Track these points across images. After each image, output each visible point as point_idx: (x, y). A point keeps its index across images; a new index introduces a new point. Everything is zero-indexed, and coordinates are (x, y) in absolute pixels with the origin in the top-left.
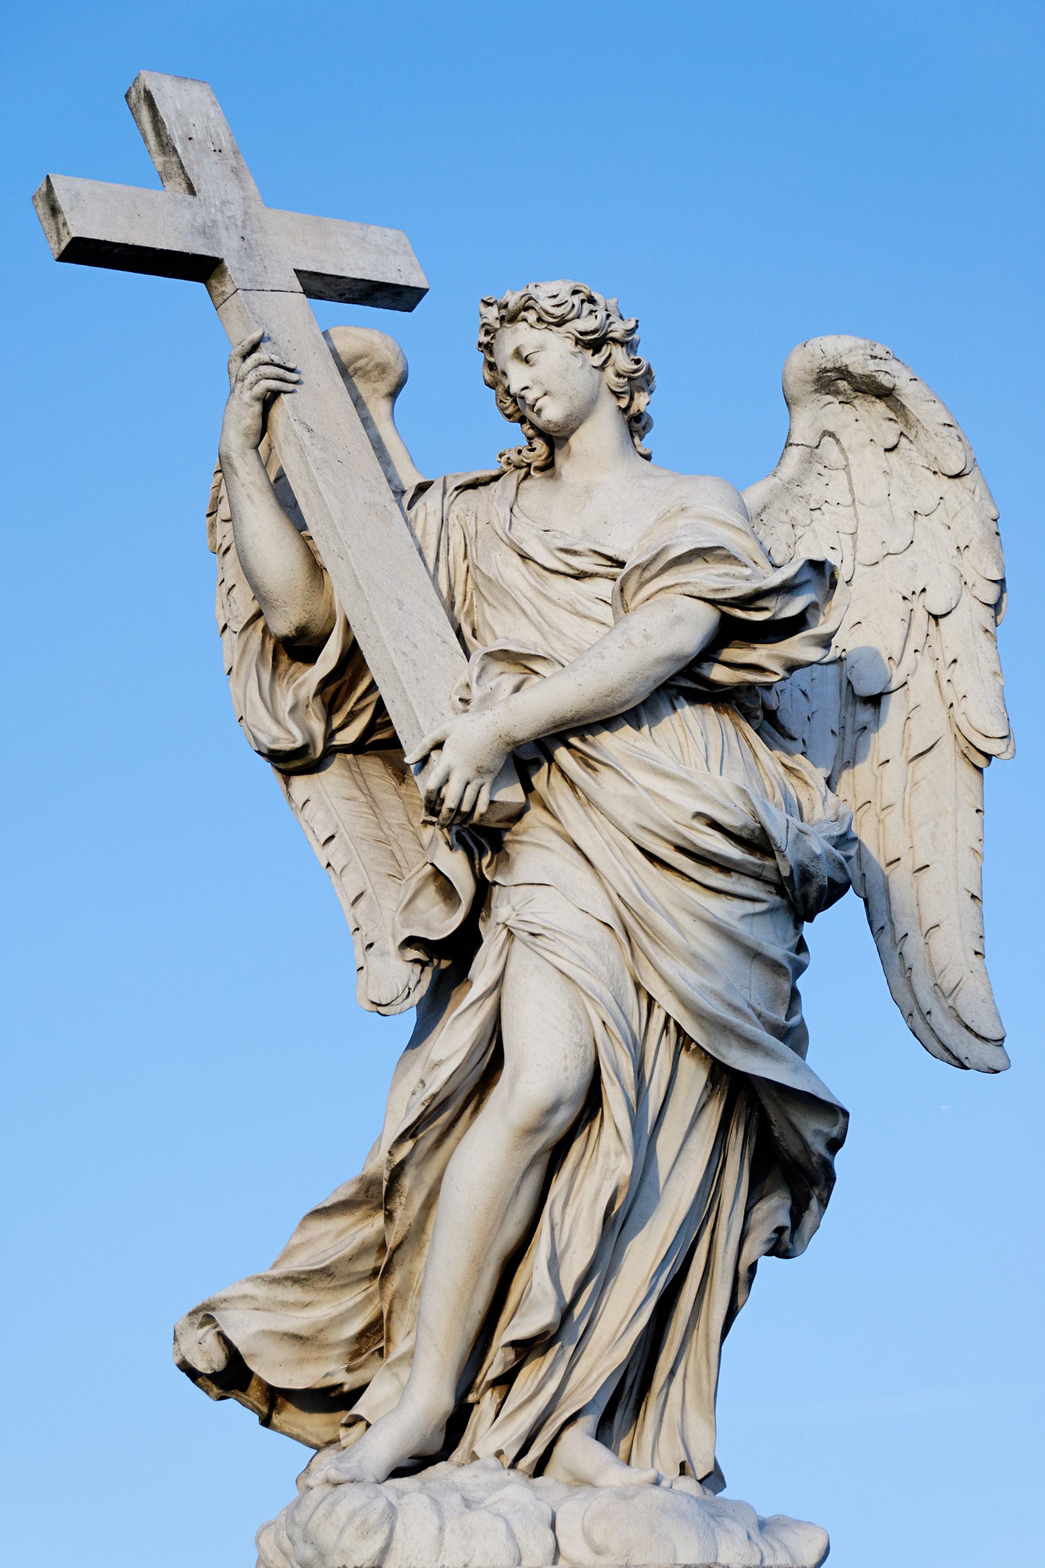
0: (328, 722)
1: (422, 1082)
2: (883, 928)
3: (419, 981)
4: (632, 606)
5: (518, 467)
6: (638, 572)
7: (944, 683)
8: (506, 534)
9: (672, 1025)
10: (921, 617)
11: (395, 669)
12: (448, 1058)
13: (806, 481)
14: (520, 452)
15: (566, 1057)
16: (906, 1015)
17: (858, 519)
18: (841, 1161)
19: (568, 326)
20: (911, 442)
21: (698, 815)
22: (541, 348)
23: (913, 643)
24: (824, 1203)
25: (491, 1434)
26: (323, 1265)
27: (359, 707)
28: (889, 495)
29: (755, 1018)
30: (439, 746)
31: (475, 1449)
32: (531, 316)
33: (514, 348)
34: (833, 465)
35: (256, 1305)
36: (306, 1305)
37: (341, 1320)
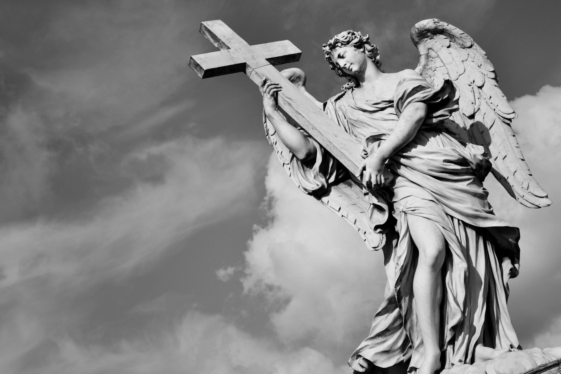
0: (326, 178)
1: (397, 264)
3: (383, 238)
4: (401, 111)
5: (349, 89)
6: (400, 100)
7: (490, 104)
8: (356, 106)
9: (460, 222)
10: (476, 89)
11: (342, 153)
17: (447, 69)
19: (351, 43)
20: (454, 42)
21: (445, 161)
22: (345, 52)
23: (477, 96)
25: (455, 356)
26: (386, 328)
30: (364, 169)
32: (339, 44)
33: (338, 55)
34: (434, 56)
35: (370, 347)
36: (384, 342)
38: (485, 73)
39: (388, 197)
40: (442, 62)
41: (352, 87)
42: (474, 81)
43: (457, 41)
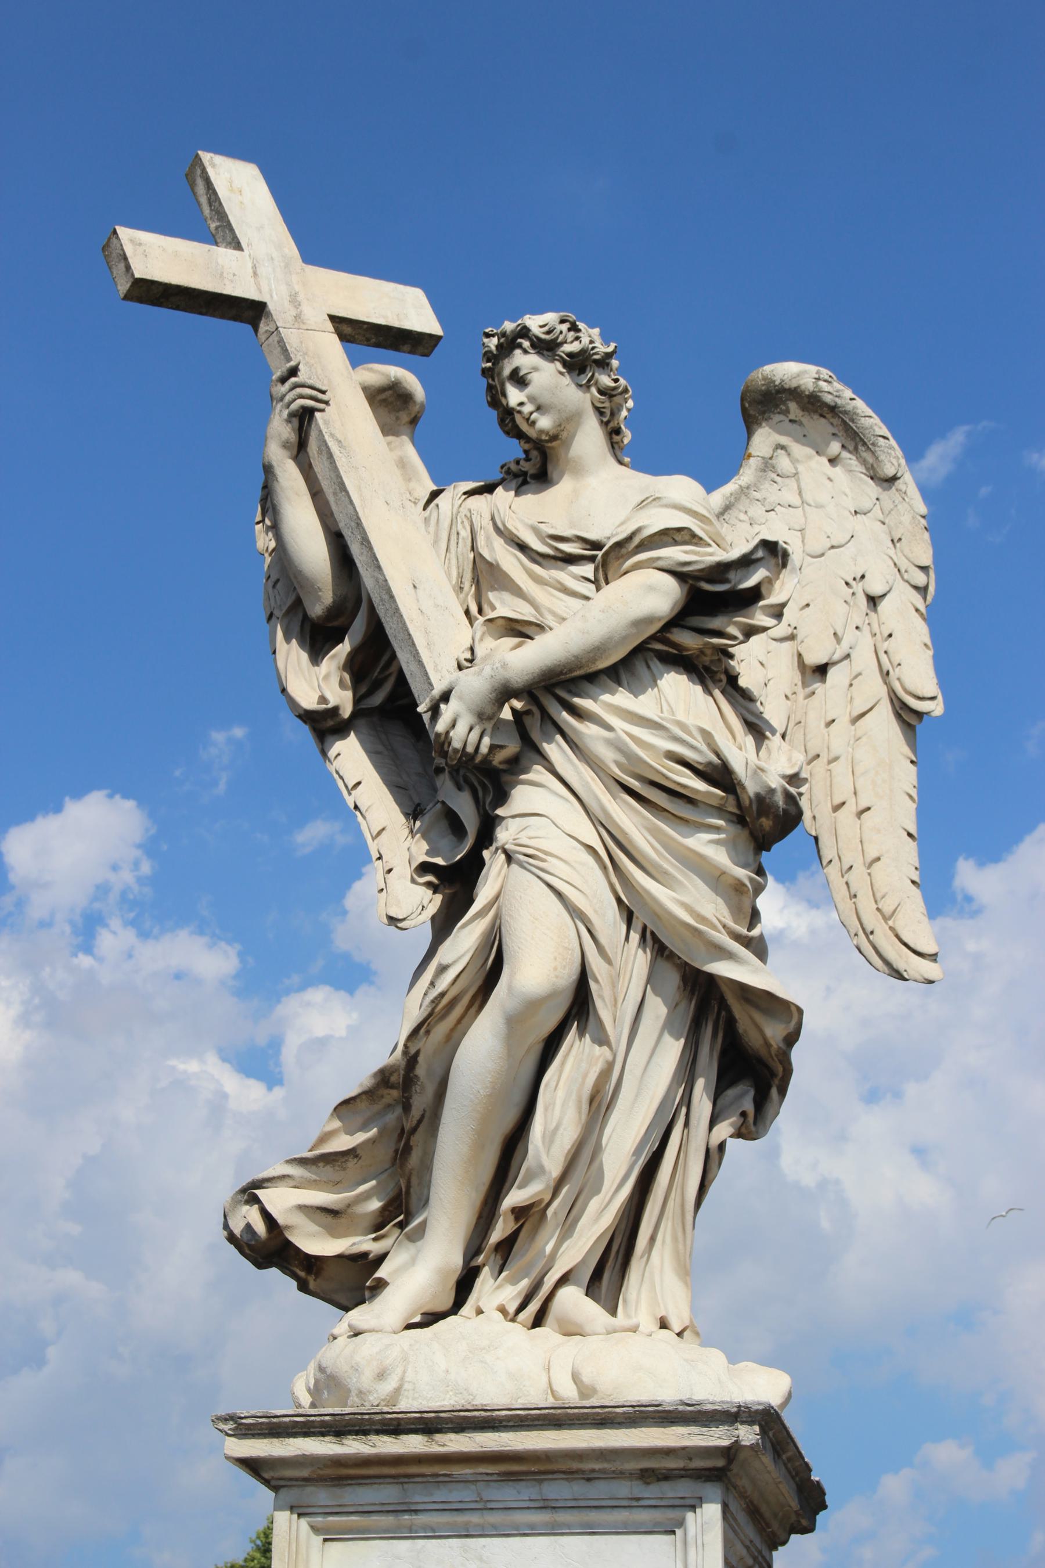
2: (831, 861)
10: (863, 601)
12: (455, 962)
13: (762, 487)
14: (518, 462)
15: (555, 959)
16: (852, 935)
18: (797, 1054)
22: (536, 369)
24: (783, 1092)
27: (383, 676)
28: (833, 497)
29: (720, 927)
30: (445, 697)
31: (481, 1304)
37: (366, 1197)
38: (904, 564)
39: (488, 800)
40: (800, 493)
41: (525, 474)
42: (863, 577)
43: (861, 453)
